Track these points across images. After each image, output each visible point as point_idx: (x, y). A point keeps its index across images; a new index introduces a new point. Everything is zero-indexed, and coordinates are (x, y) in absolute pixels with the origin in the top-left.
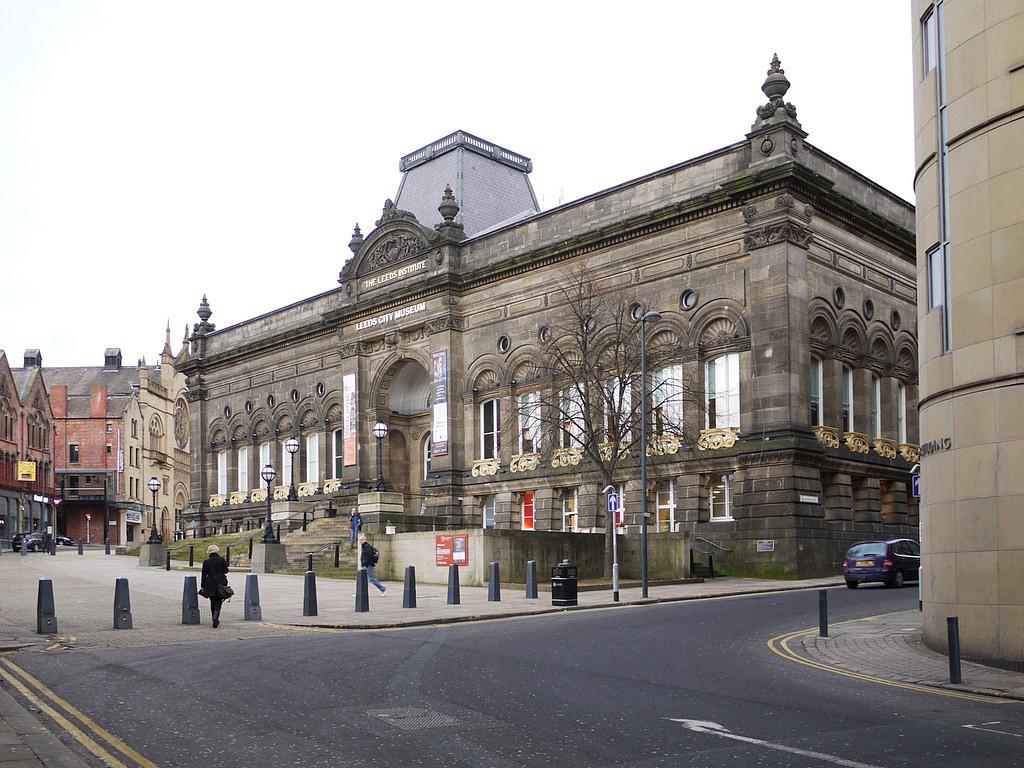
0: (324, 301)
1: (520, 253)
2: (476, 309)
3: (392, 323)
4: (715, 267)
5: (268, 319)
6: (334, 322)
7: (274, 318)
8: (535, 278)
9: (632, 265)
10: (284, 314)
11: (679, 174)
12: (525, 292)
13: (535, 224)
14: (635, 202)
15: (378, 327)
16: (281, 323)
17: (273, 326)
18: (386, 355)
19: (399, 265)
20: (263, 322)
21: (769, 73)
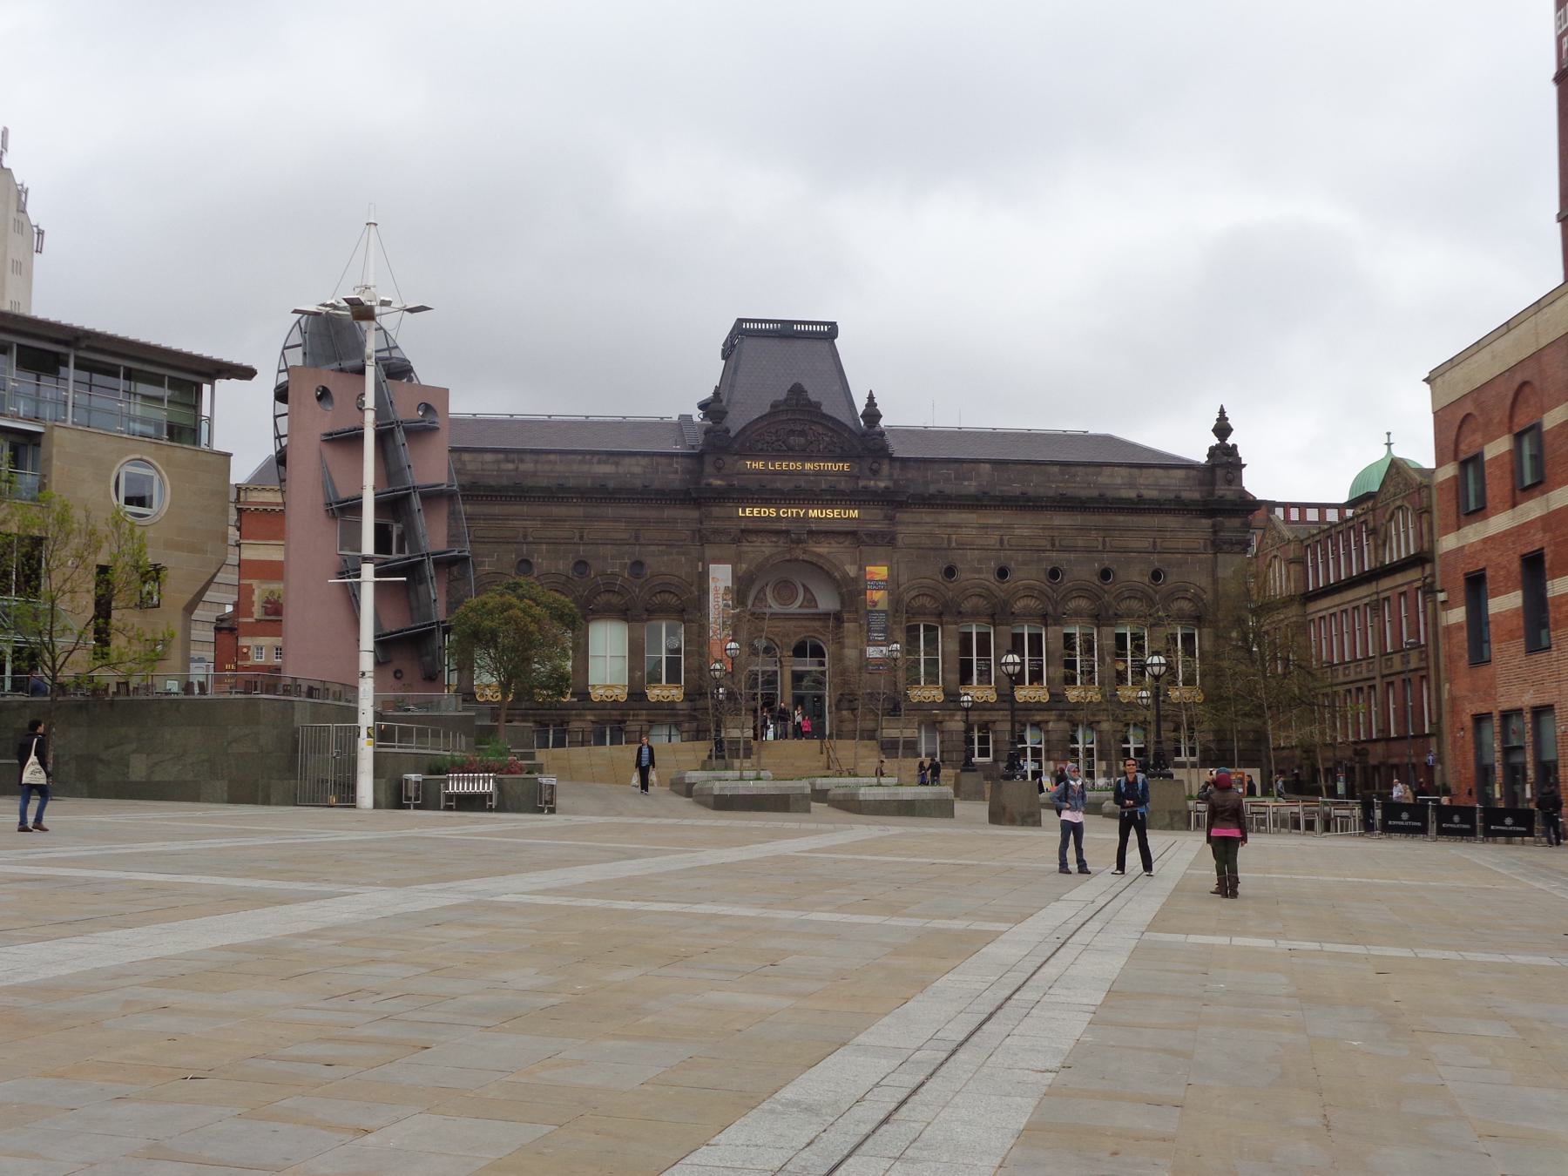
0: (644, 461)
2: (912, 529)
3: (806, 518)
5: (512, 456)
6: (695, 496)
7: (528, 457)
8: (995, 518)
9: (1102, 534)
10: (552, 457)
11: (1144, 471)
14: (1101, 480)
15: (778, 518)
16: (547, 467)
19: (810, 459)
20: (501, 456)
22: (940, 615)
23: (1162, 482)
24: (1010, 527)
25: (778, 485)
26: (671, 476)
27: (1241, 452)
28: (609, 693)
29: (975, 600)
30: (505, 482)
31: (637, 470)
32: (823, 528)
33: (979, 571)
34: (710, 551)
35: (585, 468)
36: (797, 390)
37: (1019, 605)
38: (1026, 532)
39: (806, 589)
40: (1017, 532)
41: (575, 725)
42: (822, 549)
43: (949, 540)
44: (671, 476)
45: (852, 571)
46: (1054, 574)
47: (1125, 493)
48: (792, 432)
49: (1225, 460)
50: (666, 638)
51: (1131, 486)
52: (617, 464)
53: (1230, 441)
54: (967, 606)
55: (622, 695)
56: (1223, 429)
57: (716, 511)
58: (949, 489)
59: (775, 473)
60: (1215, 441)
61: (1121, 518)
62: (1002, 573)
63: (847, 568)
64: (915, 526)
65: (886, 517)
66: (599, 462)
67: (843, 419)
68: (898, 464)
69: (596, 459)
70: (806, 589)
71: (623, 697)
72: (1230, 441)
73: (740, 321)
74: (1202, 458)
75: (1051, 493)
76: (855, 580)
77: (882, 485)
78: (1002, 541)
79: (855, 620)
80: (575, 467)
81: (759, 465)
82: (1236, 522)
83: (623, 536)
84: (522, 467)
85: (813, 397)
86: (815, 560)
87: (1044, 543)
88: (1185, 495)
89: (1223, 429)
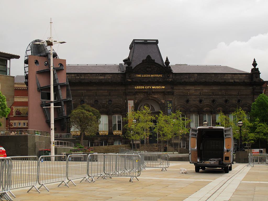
0: (111, 75)
1: (193, 81)
4: (244, 96)
5: (78, 75)
7: (83, 75)
11: (236, 75)
12: (195, 90)
13: (196, 75)
14: (225, 77)
15: (145, 89)
16: (87, 77)
17: (81, 77)
20: (76, 75)
21: (253, 62)
22: (185, 112)
23: (240, 78)
25: (144, 81)
26: (118, 79)
27: (259, 70)
28: (104, 133)
30: (77, 81)
31: (109, 77)
32: (155, 91)
33: (195, 101)
34: (128, 97)
35: (97, 77)
36: (149, 57)
38: (206, 91)
40: (204, 91)
41: (96, 141)
42: (156, 96)
43: (187, 93)
44: (118, 79)
45: (163, 101)
46: (213, 101)
47: (231, 81)
48: (148, 67)
49: (255, 72)
50: (117, 118)
51: (232, 79)
52: (104, 76)
53: (257, 67)
54: (192, 110)
55: (107, 133)
56: (255, 64)
57: (129, 87)
58: (187, 80)
59: (144, 77)
60: (253, 67)
61: (230, 87)
62: (201, 101)
63: (162, 101)
64: (178, 90)
66: (100, 76)
67: (160, 64)
68: (174, 75)
69: (99, 75)
71: (107, 134)
72: (257, 67)
73: (134, 40)
74: (250, 72)
75: (212, 81)
77: (170, 80)
78: (200, 93)
80: (94, 77)
81: (140, 76)
82: (259, 87)
83: (107, 94)
84: (81, 77)
85: (153, 58)
86: (154, 99)
87: (211, 93)
88: (245, 81)
89: (255, 64)
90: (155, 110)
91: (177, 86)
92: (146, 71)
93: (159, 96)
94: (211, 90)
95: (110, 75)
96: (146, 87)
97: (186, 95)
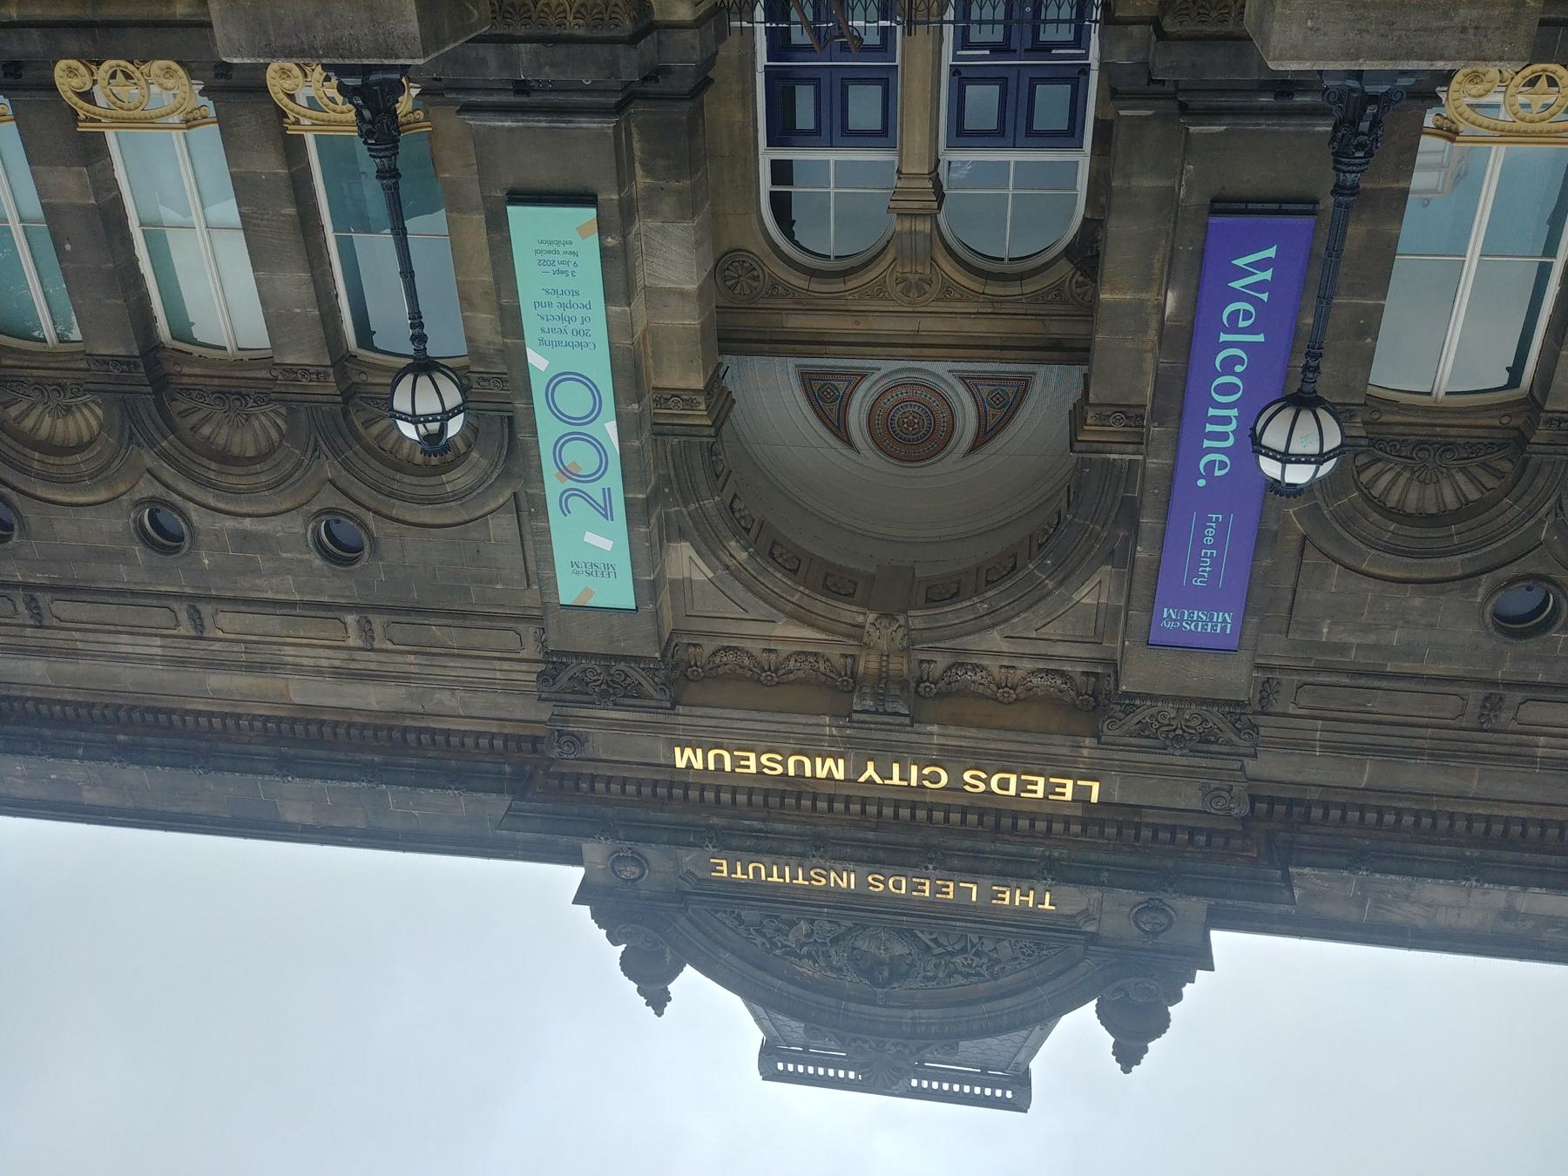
13: (291, 816)
18: (994, 640)
24: (181, 662)
29: (245, 442)
33: (244, 537)
37: (85, 420)
38: (124, 644)
39: (839, 429)
40: (155, 647)
43: (366, 630)
45: (684, 561)
52: (1508, 914)
54: (264, 425)
65: (578, 740)
70: (839, 429)
76: (671, 532)
79: (664, 396)
83: (1535, 713)
86: (821, 605)
87: (64, 609)
90: (806, 378)
91: (509, 729)
92: (925, 938)
93: (754, 628)
94: (72, 654)
95: (1421, 922)
96: (935, 778)
97: (378, 621)
